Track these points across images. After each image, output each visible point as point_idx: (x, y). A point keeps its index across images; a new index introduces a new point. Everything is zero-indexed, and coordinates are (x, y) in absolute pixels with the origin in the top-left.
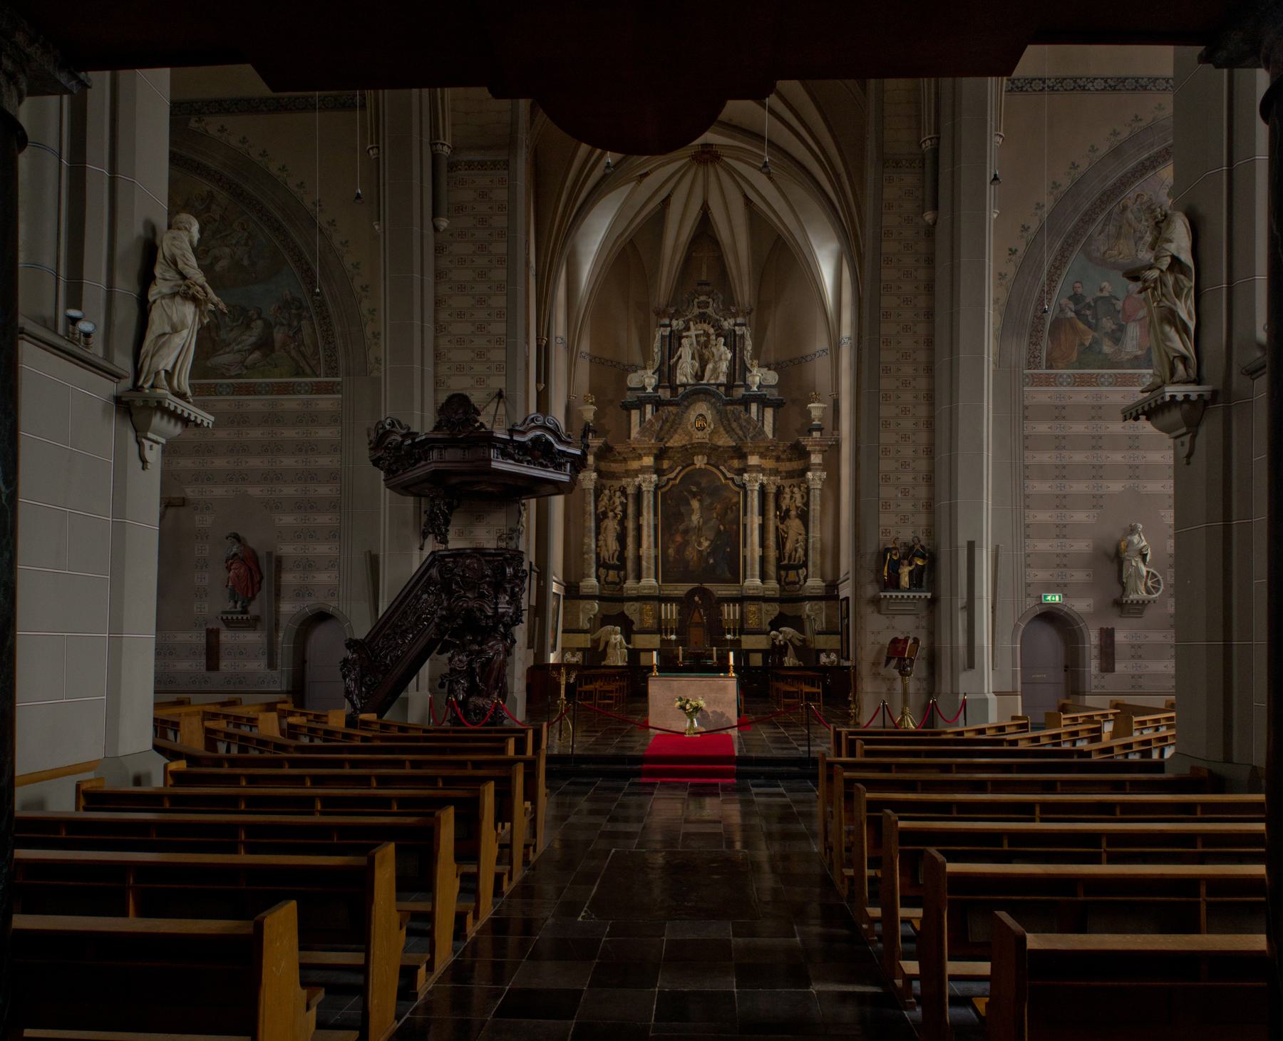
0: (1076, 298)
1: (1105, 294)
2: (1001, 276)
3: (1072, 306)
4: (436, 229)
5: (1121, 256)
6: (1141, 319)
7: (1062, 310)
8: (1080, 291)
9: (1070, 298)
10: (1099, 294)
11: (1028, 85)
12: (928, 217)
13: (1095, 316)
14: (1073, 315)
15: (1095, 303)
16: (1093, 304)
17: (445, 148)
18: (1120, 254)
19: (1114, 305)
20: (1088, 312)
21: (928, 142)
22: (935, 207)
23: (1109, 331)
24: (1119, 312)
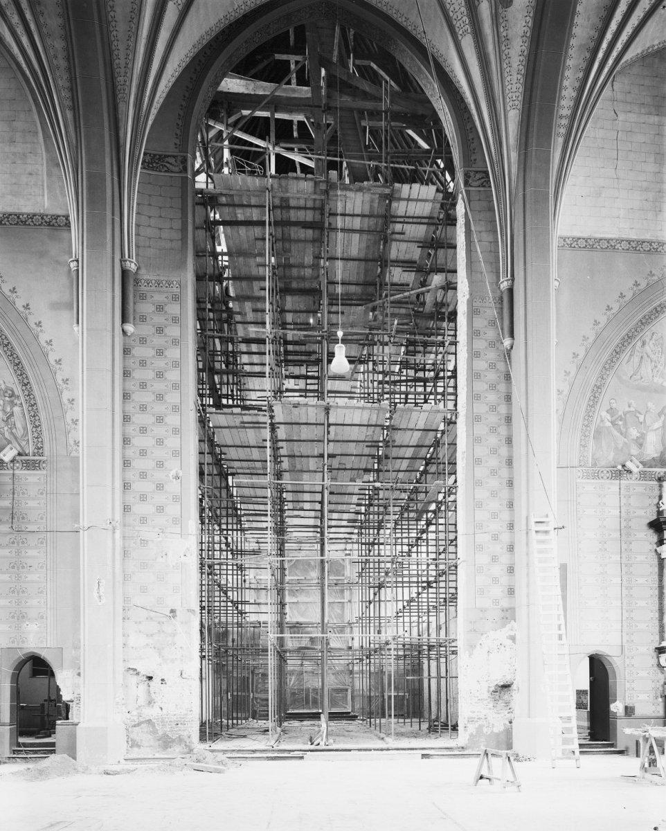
0: (611, 411)
1: (632, 409)
2: (560, 392)
3: (609, 418)
4: (124, 332)
5: (643, 380)
6: (656, 430)
7: (602, 421)
8: (614, 406)
9: (607, 412)
10: (627, 409)
11: (597, 244)
12: (507, 342)
13: (625, 424)
14: (610, 424)
15: (625, 415)
16: (623, 416)
17: (133, 264)
18: (642, 378)
19: (638, 418)
20: (620, 423)
21: (505, 283)
22: (512, 335)
23: (635, 438)
24: (641, 423)
